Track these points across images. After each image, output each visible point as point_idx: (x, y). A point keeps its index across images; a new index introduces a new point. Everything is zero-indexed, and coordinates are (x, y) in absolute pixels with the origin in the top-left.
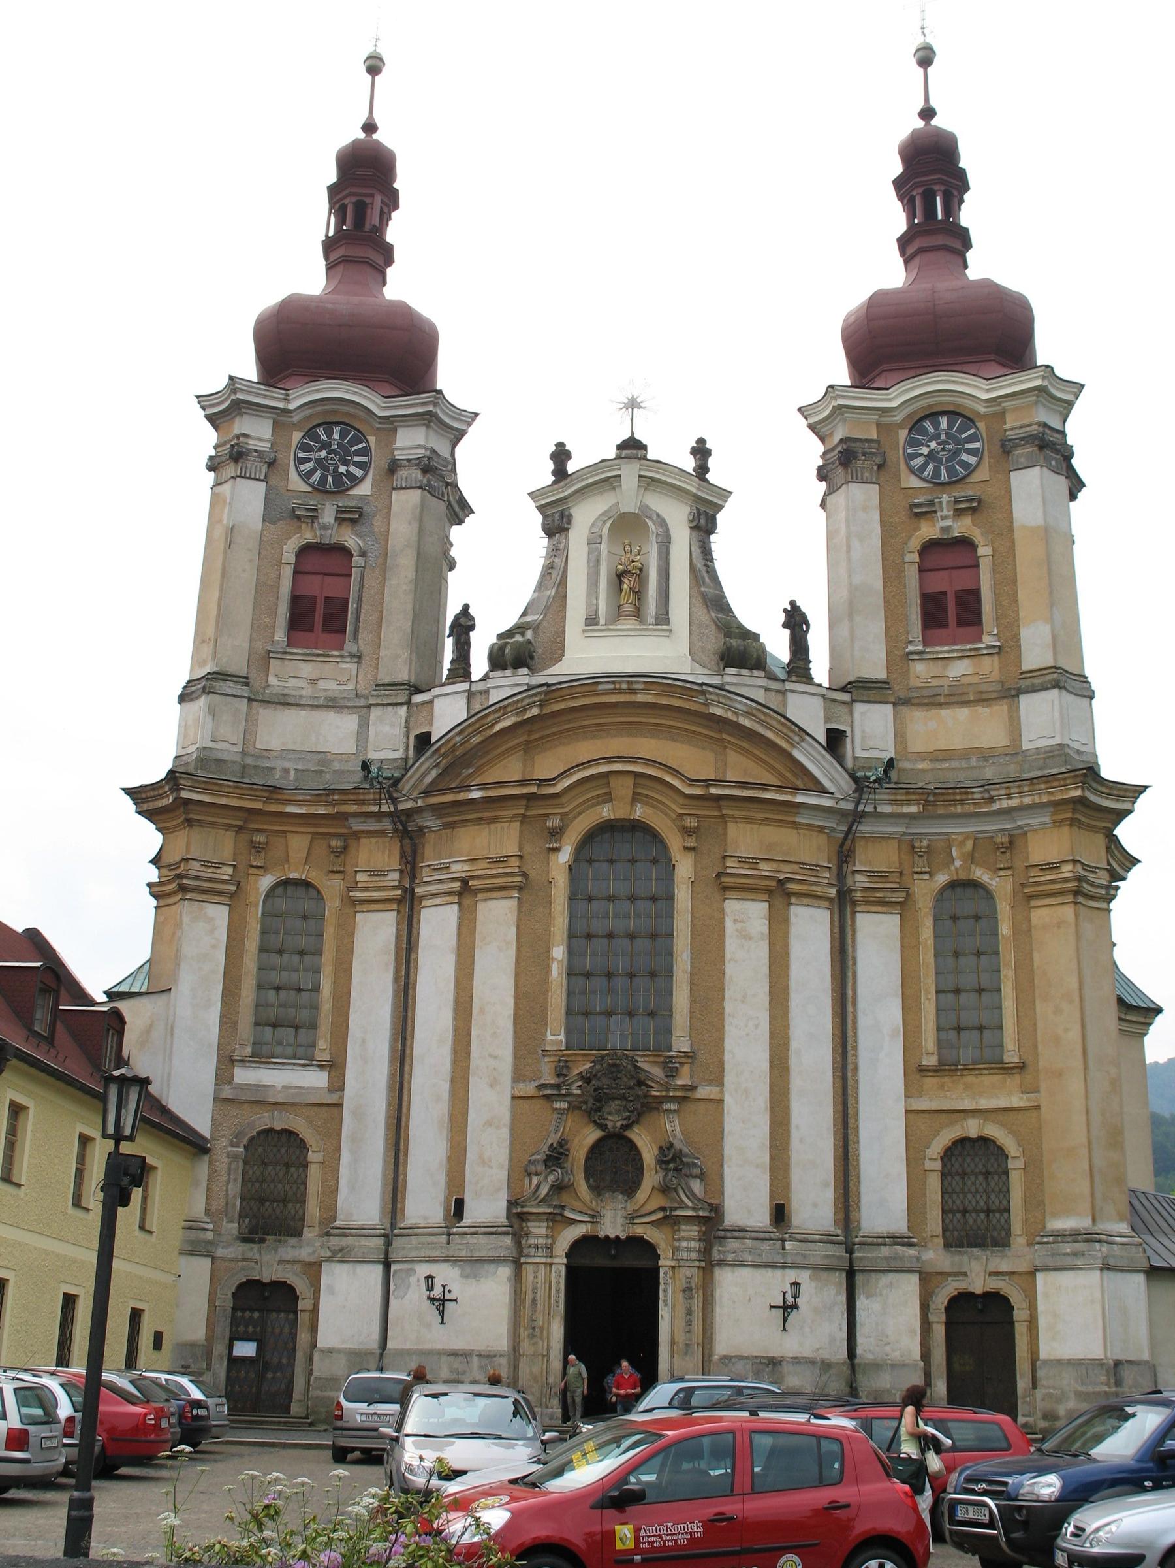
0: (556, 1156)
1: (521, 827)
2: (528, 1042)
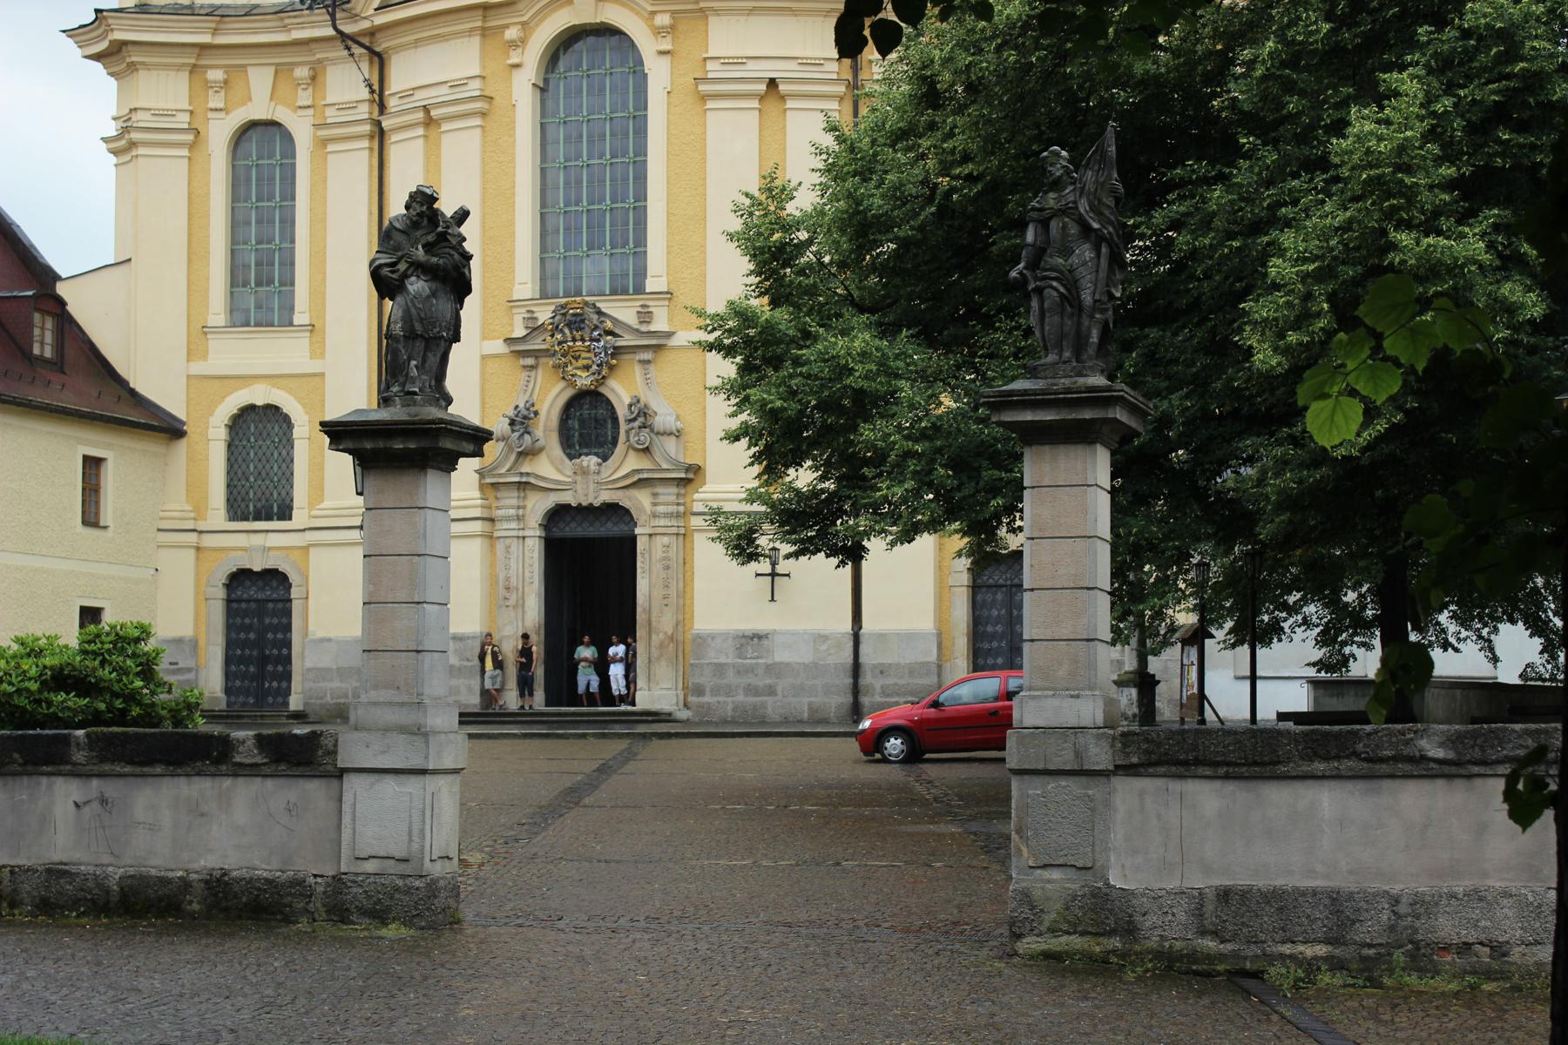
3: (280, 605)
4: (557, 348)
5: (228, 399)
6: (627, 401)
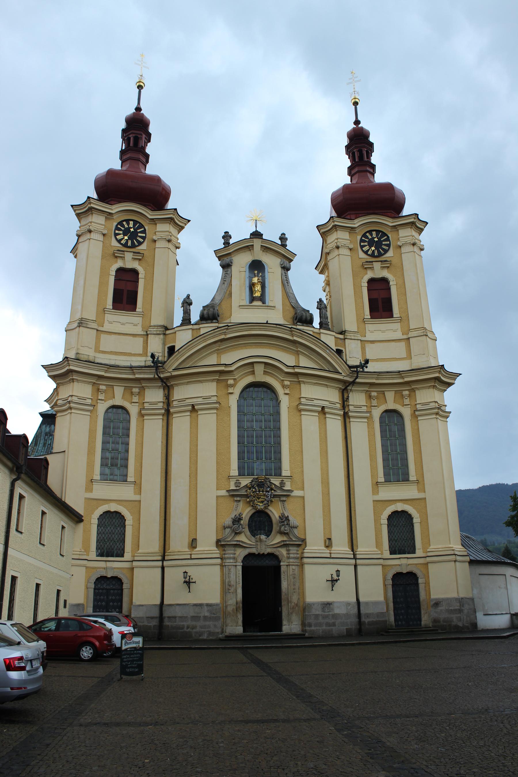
0: (237, 520)
1: (217, 385)
2: (223, 473)
3: (116, 591)
4: (252, 494)
5: (99, 508)
6: (277, 516)
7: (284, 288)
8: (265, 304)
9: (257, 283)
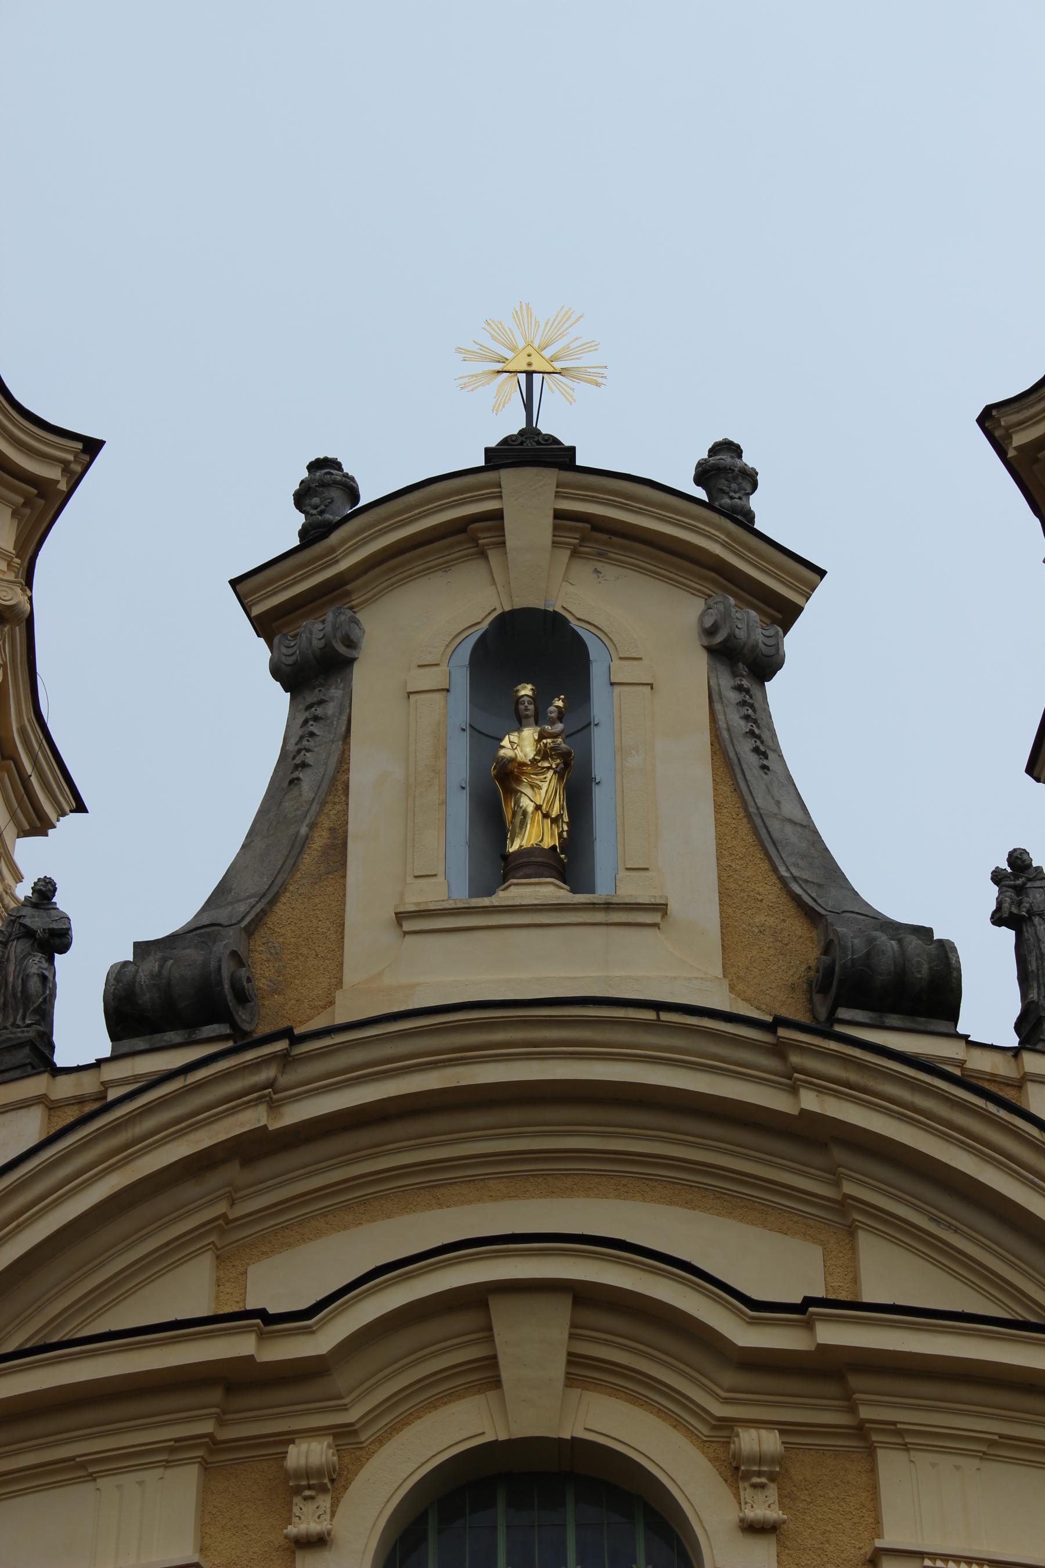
7: (737, 789)
8: (592, 891)
9: (534, 761)
